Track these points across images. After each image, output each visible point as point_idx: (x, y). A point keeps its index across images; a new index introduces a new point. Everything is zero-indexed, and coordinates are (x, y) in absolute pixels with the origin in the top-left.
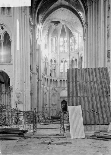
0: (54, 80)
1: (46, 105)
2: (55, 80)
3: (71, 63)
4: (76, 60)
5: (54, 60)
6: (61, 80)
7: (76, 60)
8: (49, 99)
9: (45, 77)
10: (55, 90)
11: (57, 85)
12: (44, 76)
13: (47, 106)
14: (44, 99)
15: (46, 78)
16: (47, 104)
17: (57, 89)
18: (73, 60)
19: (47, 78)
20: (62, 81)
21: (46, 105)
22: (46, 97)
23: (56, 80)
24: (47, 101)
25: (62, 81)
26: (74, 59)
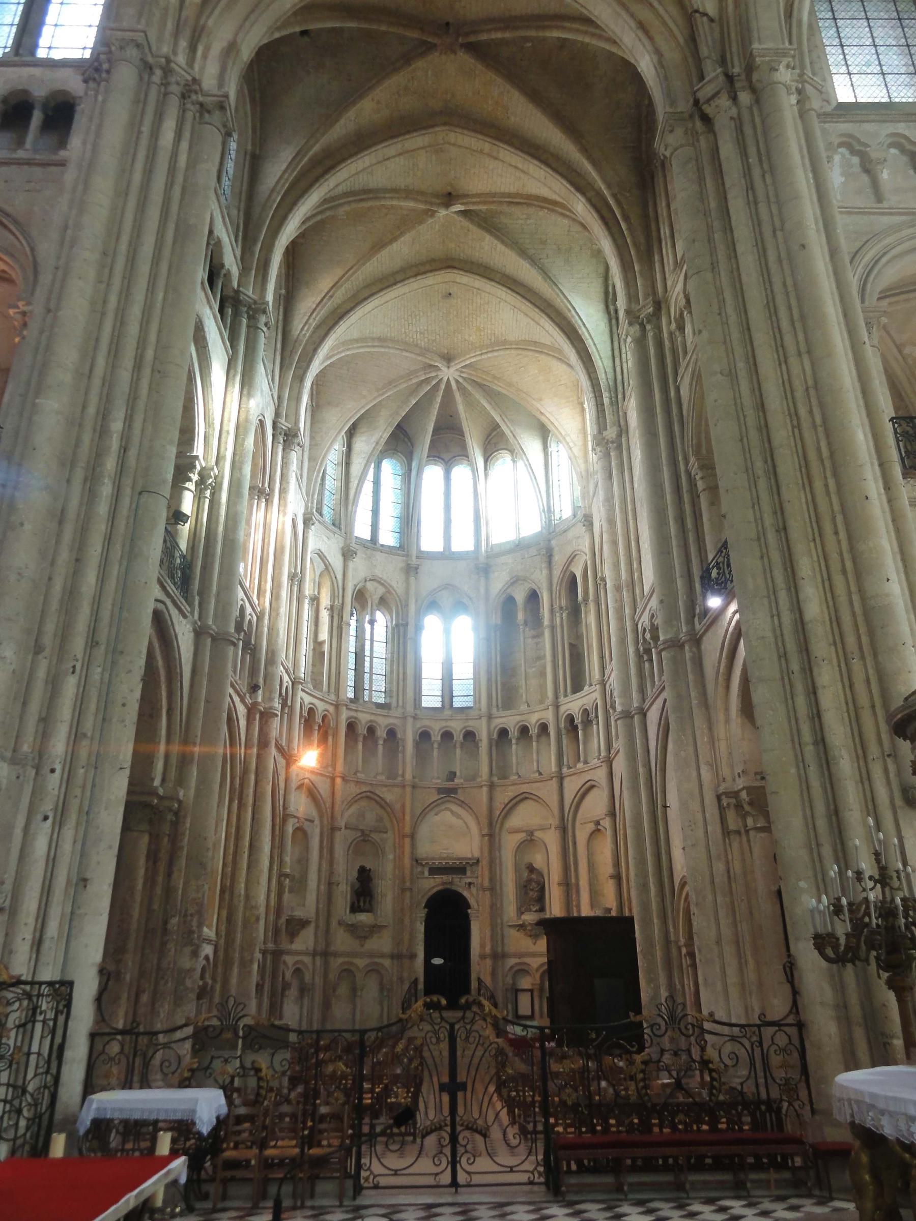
0: (371, 730)
1: (296, 926)
2: (381, 733)
3: (497, 619)
4: (533, 597)
5: (381, 590)
6: (425, 735)
7: (533, 597)
8: (331, 873)
9: (308, 699)
10: (382, 804)
11: (392, 775)
12: (300, 694)
13: (305, 940)
14: (282, 875)
15: (311, 711)
16: (303, 924)
17: (389, 796)
18: (510, 601)
19: (321, 706)
20: (436, 737)
21: (296, 926)
22: (303, 861)
23: (392, 733)
24: (311, 897)
25: (436, 737)
26: (520, 597)
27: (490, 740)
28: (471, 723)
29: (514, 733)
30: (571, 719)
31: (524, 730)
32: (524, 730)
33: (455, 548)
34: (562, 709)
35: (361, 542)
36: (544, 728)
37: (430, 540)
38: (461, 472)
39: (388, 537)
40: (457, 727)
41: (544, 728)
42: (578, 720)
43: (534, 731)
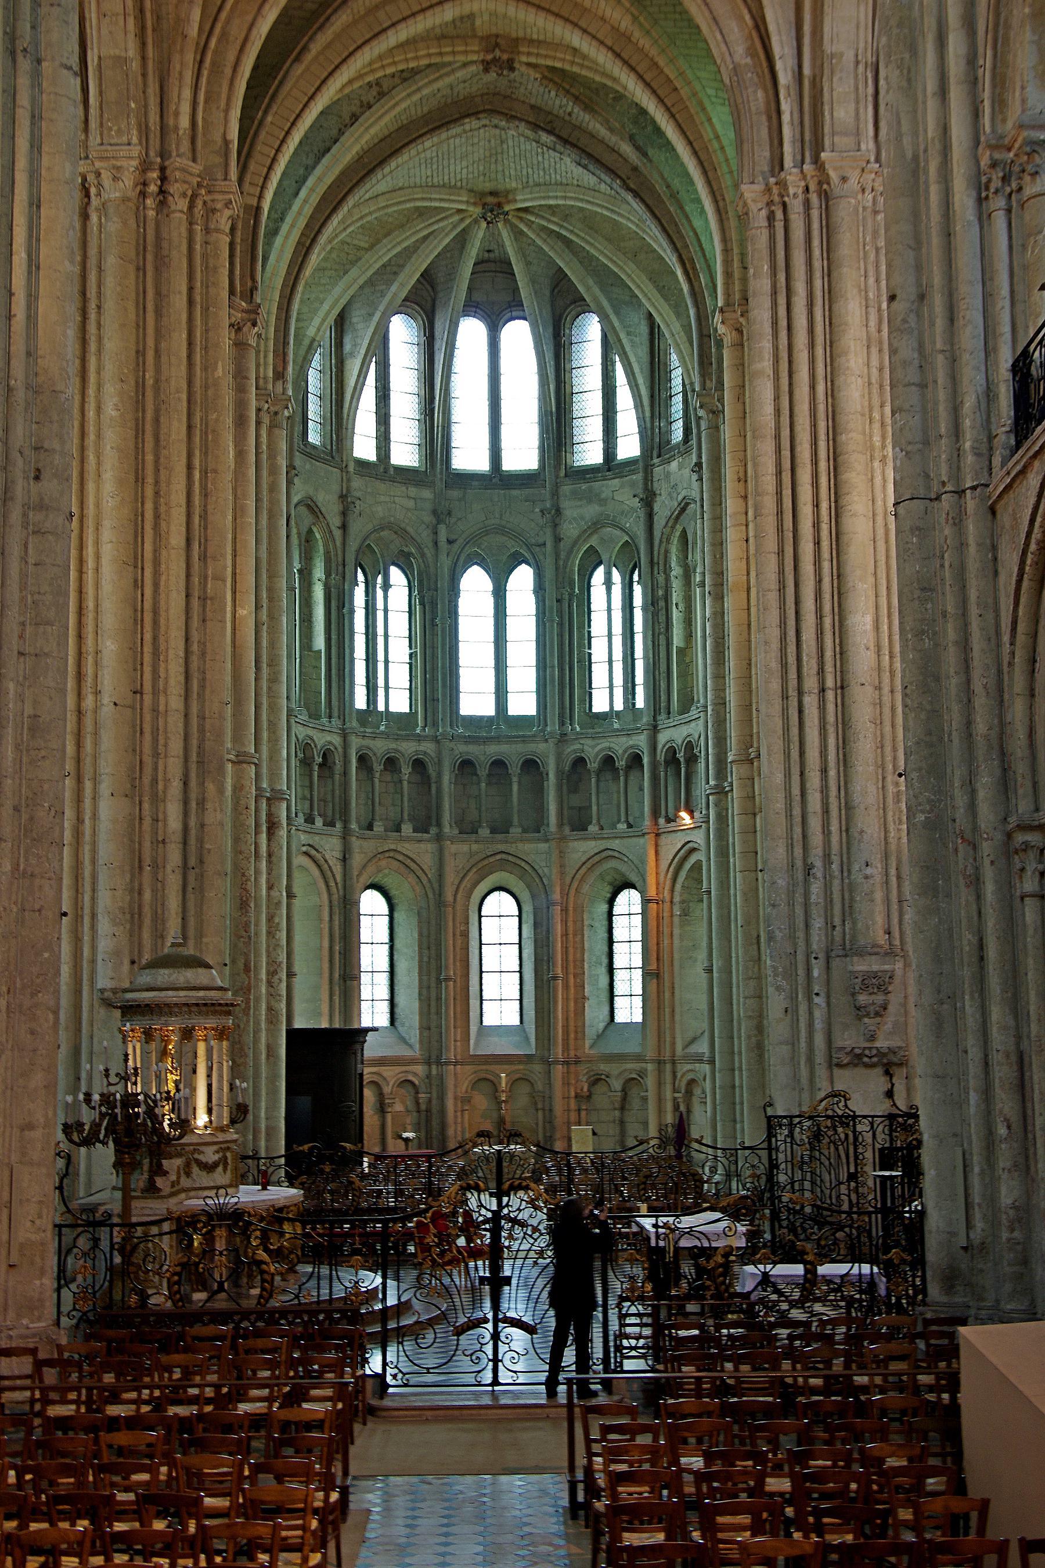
27: (559, 772)
28: (532, 747)
29: (593, 765)
30: (672, 751)
31: (608, 761)
32: (608, 761)
33: (509, 464)
34: (662, 738)
35: (362, 464)
36: (636, 760)
37: (469, 455)
38: (518, 337)
39: (405, 454)
40: (513, 753)
41: (636, 760)
42: (681, 756)
43: (621, 764)
